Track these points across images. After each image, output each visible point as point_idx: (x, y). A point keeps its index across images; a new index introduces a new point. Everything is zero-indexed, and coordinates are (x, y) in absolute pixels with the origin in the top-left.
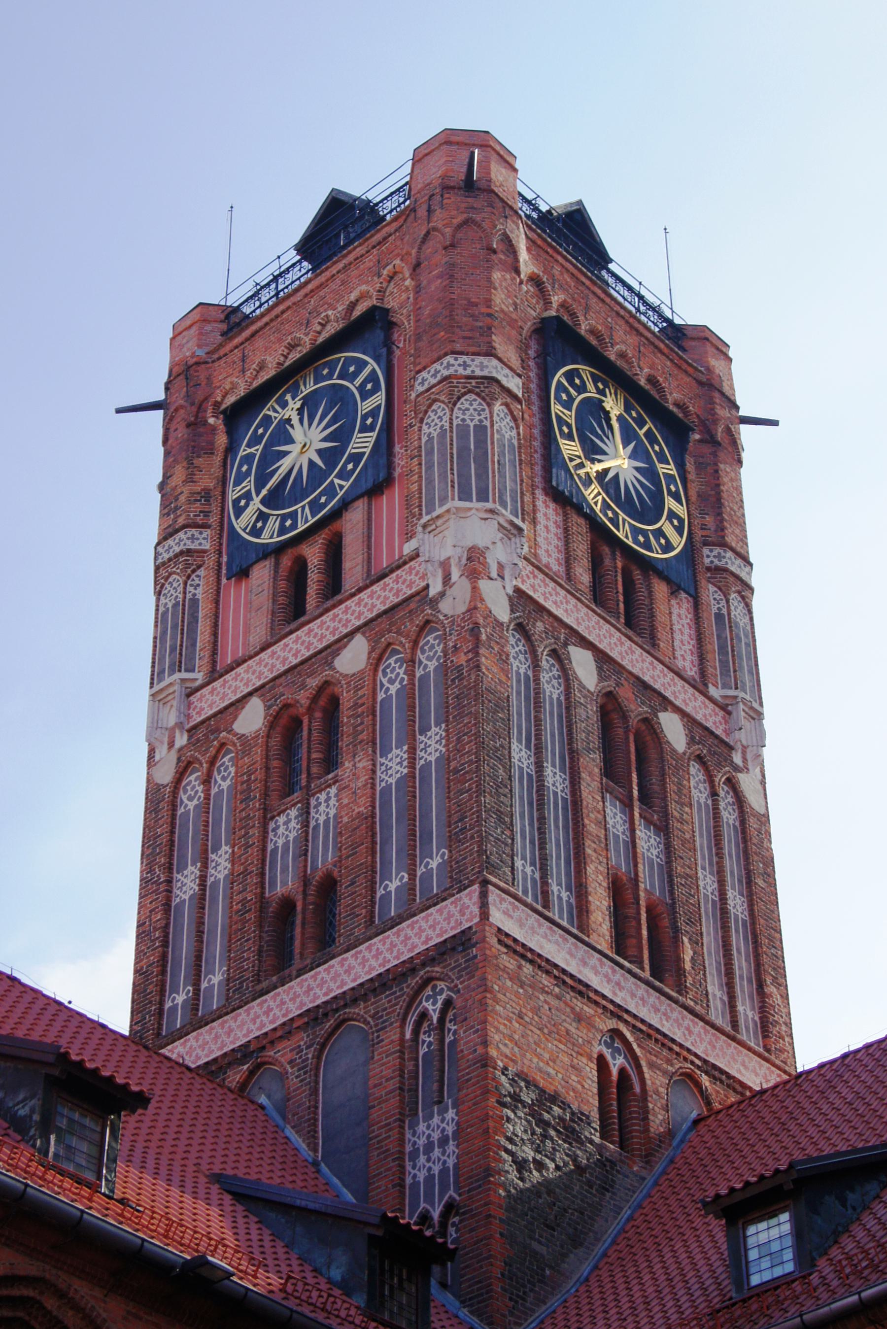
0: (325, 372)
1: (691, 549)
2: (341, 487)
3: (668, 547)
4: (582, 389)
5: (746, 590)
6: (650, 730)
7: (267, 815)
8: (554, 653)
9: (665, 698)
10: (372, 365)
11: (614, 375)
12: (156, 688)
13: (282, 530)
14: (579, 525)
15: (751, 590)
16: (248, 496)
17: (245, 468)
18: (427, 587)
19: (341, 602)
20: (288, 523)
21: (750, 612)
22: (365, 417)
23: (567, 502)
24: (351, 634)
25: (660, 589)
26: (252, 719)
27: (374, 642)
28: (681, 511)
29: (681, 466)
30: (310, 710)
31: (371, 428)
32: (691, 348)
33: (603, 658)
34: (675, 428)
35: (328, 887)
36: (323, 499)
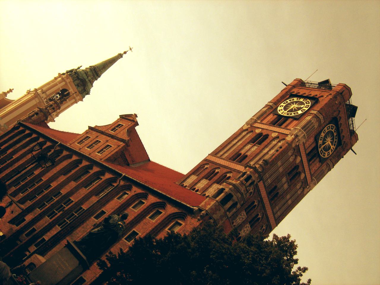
1: (327, 158)
3: (324, 156)
4: (332, 129)
5: (330, 170)
6: (299, 174)
7: (248, 143)
8: (296, 156)
9: (305, 172)
10: (310, 104)
12: (253, 118)
13: (282, 113)
15: (330, 170)
16: (283, 106)
18: (288, 135)
19: (279, 128)
21: (327, 173)
23: (316, 140)
24: (277, 132)
25: (318, 160)
26: (258, 131)
28: (331, 153)
29: (336, 148)
30: (264, 136)
32: (353, 136)
33: (302, 160)
34: (339, 143)
35: (247, 156)
36: (289, 114)
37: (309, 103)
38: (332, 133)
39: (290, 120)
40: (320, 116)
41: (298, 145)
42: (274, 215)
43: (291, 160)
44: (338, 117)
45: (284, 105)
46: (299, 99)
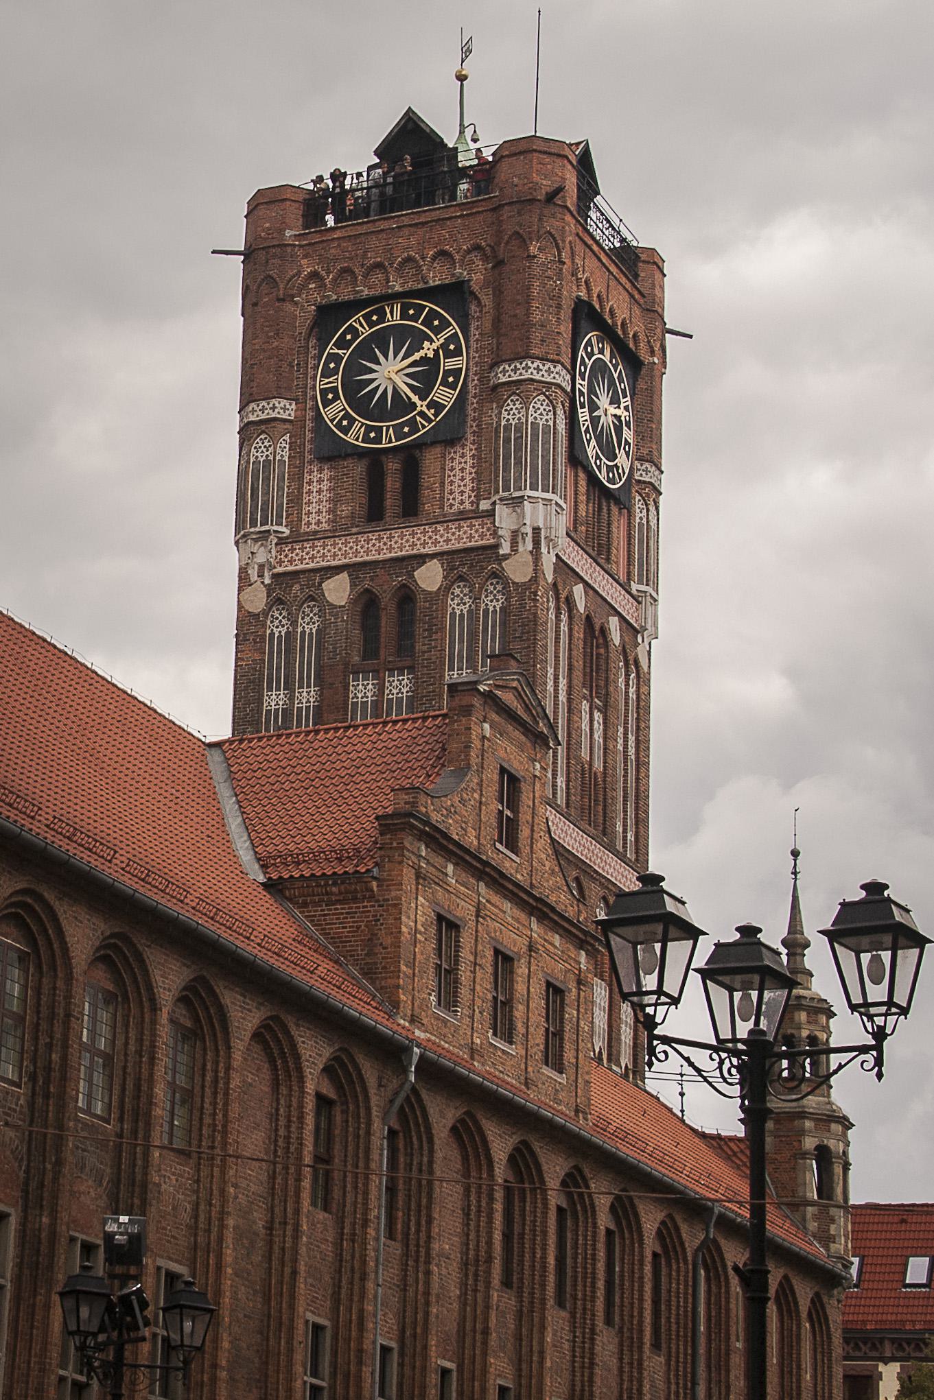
0: (411, 312)
1: (631, 468)
2: (424, 427)
10: (455, 328)
11: (609, 333)
14: (583, 483)
16: (334, 390)
17: (332, 365)
18: (497, 546)
20: (372, 435)
22: (447, 373)
23: (576, 460)
25: (615, 510)
27: (449, 569)
31: (453, 386)
32: (635, 264)
37: (445, 324)
38: (599, 367)
39: (430, 460)
40: (549, 371)
41: (557, 555)
42: (622, 857)
43: (564, 627)
44: (583, 294)
45: (337, 381)
46: (375, 318)
